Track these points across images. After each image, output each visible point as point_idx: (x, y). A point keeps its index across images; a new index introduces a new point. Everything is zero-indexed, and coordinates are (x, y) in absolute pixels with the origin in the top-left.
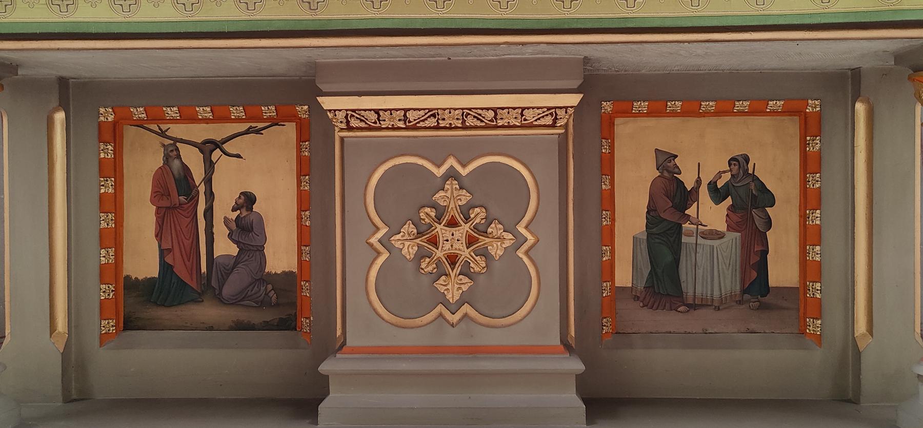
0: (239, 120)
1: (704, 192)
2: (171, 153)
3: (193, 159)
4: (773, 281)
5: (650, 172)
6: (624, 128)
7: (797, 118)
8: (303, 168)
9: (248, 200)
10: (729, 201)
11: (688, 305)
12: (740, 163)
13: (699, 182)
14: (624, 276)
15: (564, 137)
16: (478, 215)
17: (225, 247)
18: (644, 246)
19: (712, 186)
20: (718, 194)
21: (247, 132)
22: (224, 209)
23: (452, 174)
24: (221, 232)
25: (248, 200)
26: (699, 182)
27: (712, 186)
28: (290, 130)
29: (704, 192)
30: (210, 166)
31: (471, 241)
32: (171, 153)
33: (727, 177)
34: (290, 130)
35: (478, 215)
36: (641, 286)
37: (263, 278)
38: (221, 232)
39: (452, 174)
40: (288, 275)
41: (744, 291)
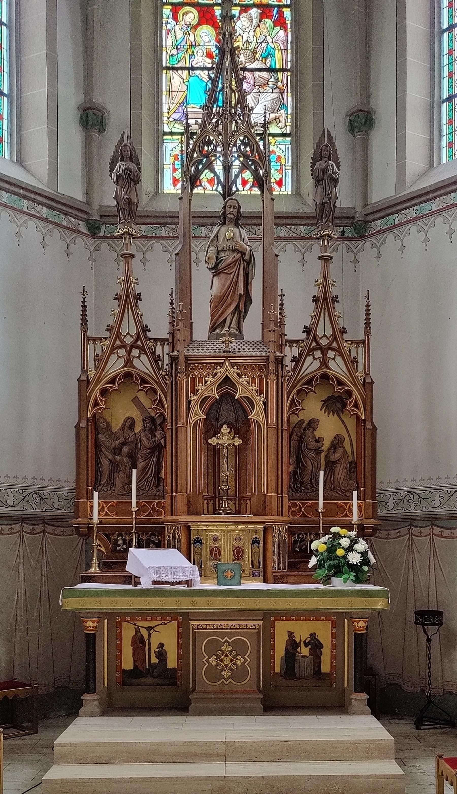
0: (159, 620)
1: (302, 644)
2: (137, 631)
3: (144, 633)
4: (322, 671)
7: (330, 622)
8: (179, 636)
9: (161, 645)
10: (310, 646)
11: (297, 678)
13: (301, 641)
14: (278, 669)
17: (154, 660)
18: (284, 660)
19: (305, 642)
20: (306, 645)
21: (161, 624)
22: (154, 648)
23: (226, 641)
24: (153, 655)
25: (161, 645)
26: (301, 641)
27: (305, 642)
28: (175, 623)
29: (302, 644)
30: (150, 635)
31: (232, 661)
33: (309, 639)
34: (175, 623)
36: (283, 672)
37: (166, 670)
38: (153, 655)
39: (226, 641)
40: (173, 669)
41: (314, 674)
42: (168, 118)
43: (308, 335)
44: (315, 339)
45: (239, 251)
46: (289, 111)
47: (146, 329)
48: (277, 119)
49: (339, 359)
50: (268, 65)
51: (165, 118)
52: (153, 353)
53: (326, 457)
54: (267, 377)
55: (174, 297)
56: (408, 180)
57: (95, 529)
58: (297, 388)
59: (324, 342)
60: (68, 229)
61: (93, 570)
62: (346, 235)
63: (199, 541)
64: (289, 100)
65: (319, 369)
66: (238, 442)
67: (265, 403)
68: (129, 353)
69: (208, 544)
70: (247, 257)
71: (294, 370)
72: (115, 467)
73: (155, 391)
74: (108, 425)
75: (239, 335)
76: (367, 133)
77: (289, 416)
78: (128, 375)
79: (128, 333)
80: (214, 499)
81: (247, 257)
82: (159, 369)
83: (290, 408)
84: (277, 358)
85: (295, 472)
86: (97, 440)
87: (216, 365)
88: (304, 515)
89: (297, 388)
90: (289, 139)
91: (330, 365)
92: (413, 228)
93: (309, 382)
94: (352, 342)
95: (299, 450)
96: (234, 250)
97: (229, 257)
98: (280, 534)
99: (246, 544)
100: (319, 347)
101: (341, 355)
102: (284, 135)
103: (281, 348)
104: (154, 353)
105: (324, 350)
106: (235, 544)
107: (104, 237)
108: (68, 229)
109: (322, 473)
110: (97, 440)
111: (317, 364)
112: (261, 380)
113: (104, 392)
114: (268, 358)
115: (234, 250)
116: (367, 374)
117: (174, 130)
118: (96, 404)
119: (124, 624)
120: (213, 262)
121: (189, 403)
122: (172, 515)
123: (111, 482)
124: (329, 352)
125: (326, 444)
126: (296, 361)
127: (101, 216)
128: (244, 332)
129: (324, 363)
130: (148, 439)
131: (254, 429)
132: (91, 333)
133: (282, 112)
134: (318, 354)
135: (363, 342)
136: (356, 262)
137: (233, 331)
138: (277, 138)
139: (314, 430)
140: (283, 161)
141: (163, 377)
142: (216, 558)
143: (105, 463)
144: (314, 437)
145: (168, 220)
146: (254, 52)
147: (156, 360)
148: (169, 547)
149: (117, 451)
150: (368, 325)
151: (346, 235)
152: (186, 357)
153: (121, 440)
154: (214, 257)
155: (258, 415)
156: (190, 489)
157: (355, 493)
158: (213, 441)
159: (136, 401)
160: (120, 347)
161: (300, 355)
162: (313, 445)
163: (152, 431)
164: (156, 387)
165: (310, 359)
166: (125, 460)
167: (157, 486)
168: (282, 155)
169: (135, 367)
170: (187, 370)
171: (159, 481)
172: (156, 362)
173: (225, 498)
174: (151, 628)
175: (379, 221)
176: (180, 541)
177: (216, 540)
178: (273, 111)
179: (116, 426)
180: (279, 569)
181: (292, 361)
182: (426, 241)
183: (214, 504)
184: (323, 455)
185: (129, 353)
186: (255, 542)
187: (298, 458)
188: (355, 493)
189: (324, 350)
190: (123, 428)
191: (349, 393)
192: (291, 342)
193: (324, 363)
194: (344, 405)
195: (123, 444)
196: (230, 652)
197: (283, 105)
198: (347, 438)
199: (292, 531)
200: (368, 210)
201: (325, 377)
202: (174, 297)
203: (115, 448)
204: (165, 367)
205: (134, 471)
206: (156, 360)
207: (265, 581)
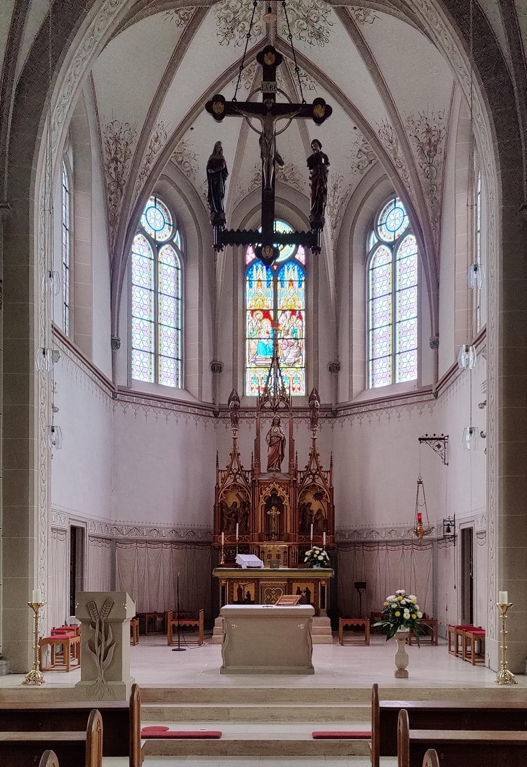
2: (239, 586)
5: (297, 589)
6: (294, 584)
9: (248, 592)
12: (307, 588)
15: (286, 587)
16: (276, 594)
17: (246, 597)
22: (246, 593)
24: (245, 595)
25: (248, 592)
28: (254, 584)
32: (239, 586)
34: (254, 584)
35: (276, 594)
38: (245, 595)
42: (249, 361)
43: (307, 469)
44: (310, 470)
45: (279, 437)
46: (304, 357)
47: (242, 467)
48: (298, 360)
49: (320, 478)
50: (294, 337)
51: (247, 361)
52: (245, 476)
53: (315, 518)
54: (290, 488)
55: (254, 453)
56: (354, 397)
57: (223, 547)
58: (303, 490)
59: (314, 472)
60: (206, 416)
61: (222, 563)
62: (328, 416)
63: (263, 552)
64: (304, 352)
65: (312, 482)
66: (278, 513)
67: (289, 498)
68: (235, 476)
69: (267, 553)
70: (282, 439)
71: (301, 483)
72: (229, 522)
73: (245, 492)
74: (226, 505)
75: (279, 471)
76: (337, 373)
77: (299, 502)
78: (235, 485)
79: (235, 469)
80: (269, 535)
81: (282, 439)
82: (248, 483)
83: (300, 498)
84: (294, 480)
85: (302, 524)
86: (222, 511)
87: (271, 483)
88: (305, 542)
89: (303, 490)
90: (304, 369)
91: (316, 481)
92: (356, 417)
93: (307, 488)
94: (325, 472)
95: (303, 516)
96: (277, 437)
97: (275, 440)
98: (295, 549)
99: (281, 553)
100: (311, 474)
101: (320, 476)
102: (301, 368)
103: (296, 476)
104: (245, 476)
105: (314, 475)
106: (277, 553)
107: (221, 417)
108: (206, 416)
109: (312, 525)
110: (222, 511)
111: (311, 480)
112: (288, 489)
113: (225, 492)
114: (290, 480)
115: (277, 437)
116: (331, 485)
117: (251, 366)
118: (222, 497)
119: (234, 584)
120: (269, 441)
121: (259, 498)
122: (252, 542)
123: (227, 528)
124: (316, 475)
125: (315, 513)
126: (302, 479)
127: (219, 409)
128: (281, 468)
129: (314, 480)
130: (243, 511)
131: (285, 508)
132: (220, 469)
133: (301, 357)
134: (311, 476)
135: (329, 471)
136: (333, 427)
137: (277, 468)
138: (298, 369)
139: (310, 507)
140: (301, 379)
141: (249, 486)
142: (269, 558)
143: (225, 521)
144: (310, 510)
145: (249, 410)
146: (288, 331)
147: (246, 479)
148: (251, 554)
149: (230, 516)
150: (331, 465)
151: (328, 416)
152: (258, 480)
153: (232, 511)
154: (269, 440)
155: (286, 502)
156: (260, 531)
157: (324, 533)
158: (269, 513)
159: (238, 495)
160: (231, 474)
161: (304, 477)
162: (309, 513)
163: (244, 507)
164: (246, 490)
165: (308, 478)
166: (234, 519)
167: (246, 530)
168: (300, 377)
169: (238, 482)
170: (259, 485)
171: (247, 528)
172: (246, 480)
173: (273, 535)
174: (245, 585)
175: (342, 411)
176: (256, 552)
177: (270, 551)
178: (296, 356)
179: (229, 506)
180: (294, 563)
181: (300, 480)
182: (361, 423)
183: (269, 537)
184: (313, 517)
185: (235, 476)
186: (285, 552)
187: (303, 517)
188: (324, 533)
189: (314, 475)
190: (232, 506)
191: (324, 492)
192: (300, 472)
193: (314, 480)
194: (322, 497)
195: (232, 513)
196: (275, 594)
197: (301, 354)
198: (323, 510)
199: (300, 548)
200: (338, 406)
201: (314, 485)
202: (254, 453)
203: (229, 514)
204: (250, 482)
205: (237, 524)
206: (246, 479)
207: (289, 567)
